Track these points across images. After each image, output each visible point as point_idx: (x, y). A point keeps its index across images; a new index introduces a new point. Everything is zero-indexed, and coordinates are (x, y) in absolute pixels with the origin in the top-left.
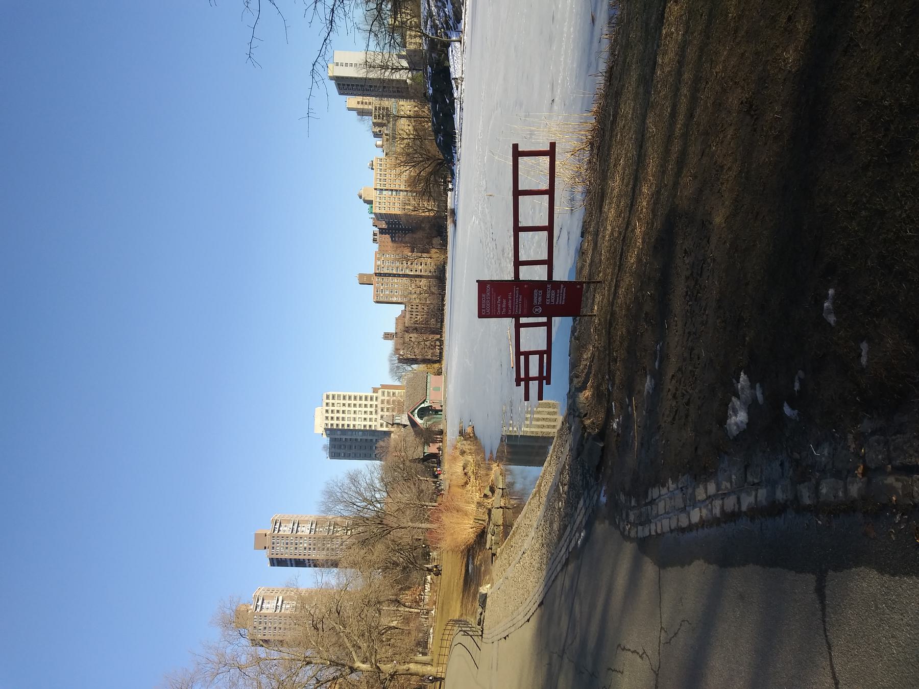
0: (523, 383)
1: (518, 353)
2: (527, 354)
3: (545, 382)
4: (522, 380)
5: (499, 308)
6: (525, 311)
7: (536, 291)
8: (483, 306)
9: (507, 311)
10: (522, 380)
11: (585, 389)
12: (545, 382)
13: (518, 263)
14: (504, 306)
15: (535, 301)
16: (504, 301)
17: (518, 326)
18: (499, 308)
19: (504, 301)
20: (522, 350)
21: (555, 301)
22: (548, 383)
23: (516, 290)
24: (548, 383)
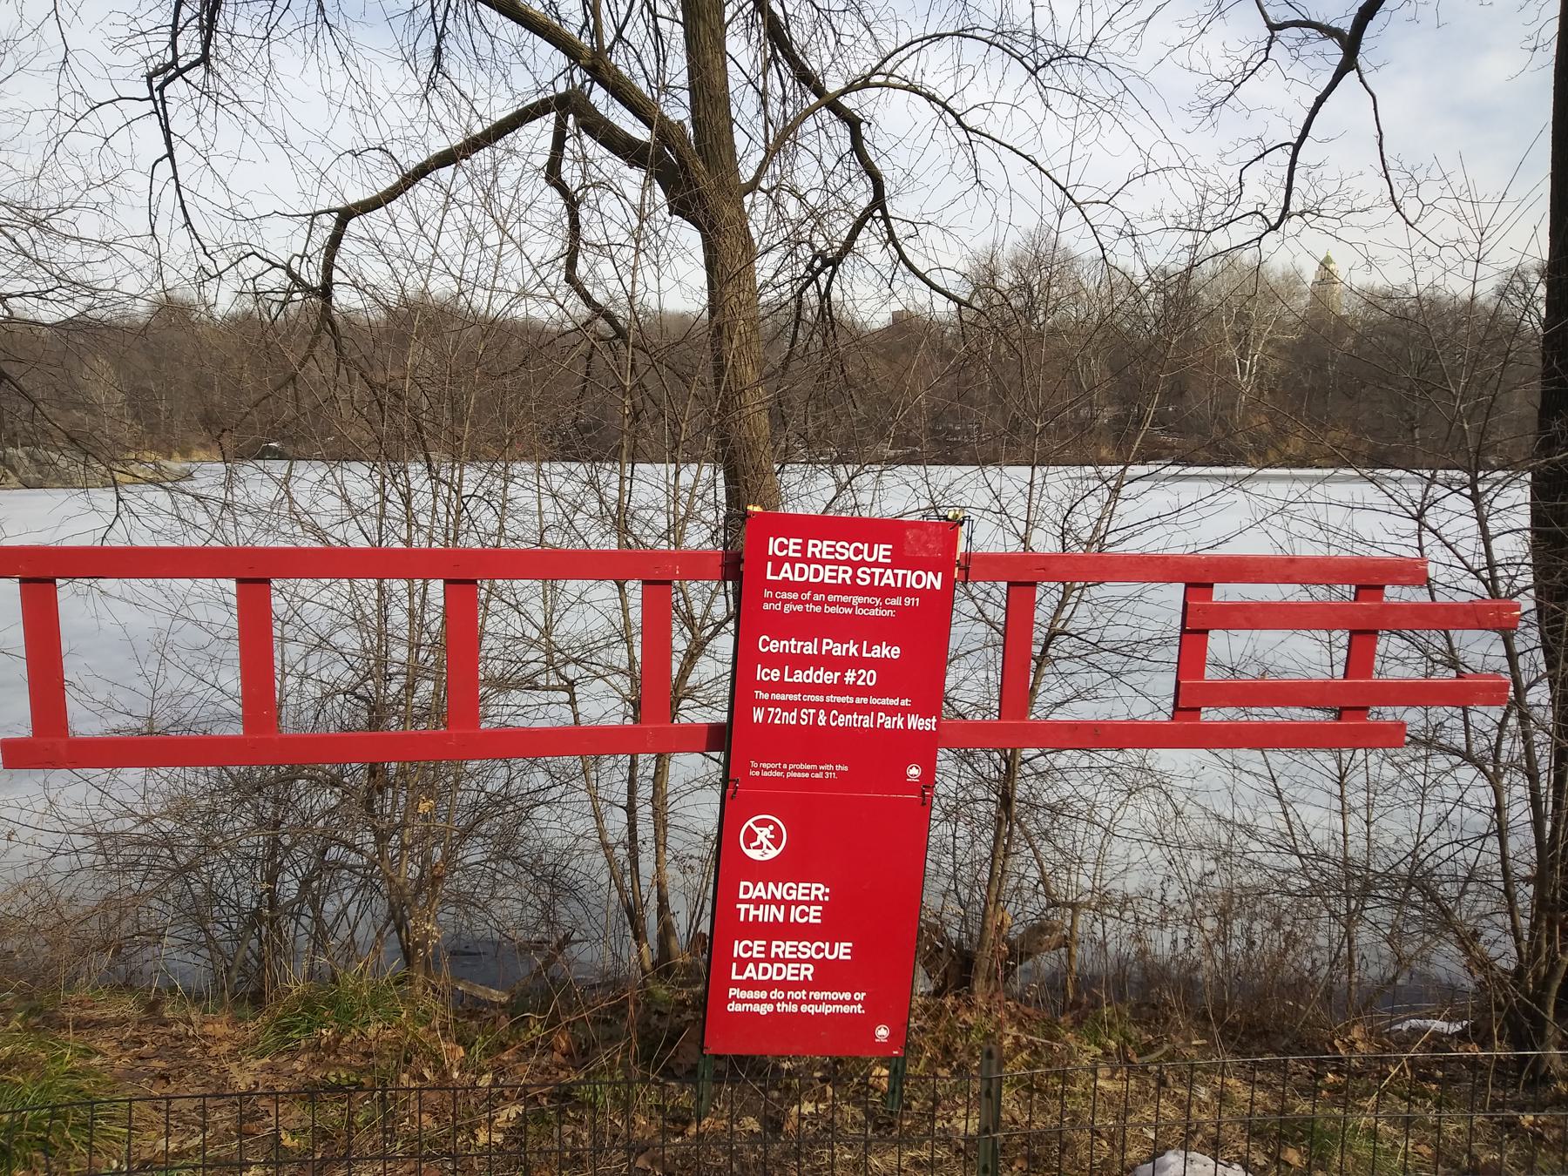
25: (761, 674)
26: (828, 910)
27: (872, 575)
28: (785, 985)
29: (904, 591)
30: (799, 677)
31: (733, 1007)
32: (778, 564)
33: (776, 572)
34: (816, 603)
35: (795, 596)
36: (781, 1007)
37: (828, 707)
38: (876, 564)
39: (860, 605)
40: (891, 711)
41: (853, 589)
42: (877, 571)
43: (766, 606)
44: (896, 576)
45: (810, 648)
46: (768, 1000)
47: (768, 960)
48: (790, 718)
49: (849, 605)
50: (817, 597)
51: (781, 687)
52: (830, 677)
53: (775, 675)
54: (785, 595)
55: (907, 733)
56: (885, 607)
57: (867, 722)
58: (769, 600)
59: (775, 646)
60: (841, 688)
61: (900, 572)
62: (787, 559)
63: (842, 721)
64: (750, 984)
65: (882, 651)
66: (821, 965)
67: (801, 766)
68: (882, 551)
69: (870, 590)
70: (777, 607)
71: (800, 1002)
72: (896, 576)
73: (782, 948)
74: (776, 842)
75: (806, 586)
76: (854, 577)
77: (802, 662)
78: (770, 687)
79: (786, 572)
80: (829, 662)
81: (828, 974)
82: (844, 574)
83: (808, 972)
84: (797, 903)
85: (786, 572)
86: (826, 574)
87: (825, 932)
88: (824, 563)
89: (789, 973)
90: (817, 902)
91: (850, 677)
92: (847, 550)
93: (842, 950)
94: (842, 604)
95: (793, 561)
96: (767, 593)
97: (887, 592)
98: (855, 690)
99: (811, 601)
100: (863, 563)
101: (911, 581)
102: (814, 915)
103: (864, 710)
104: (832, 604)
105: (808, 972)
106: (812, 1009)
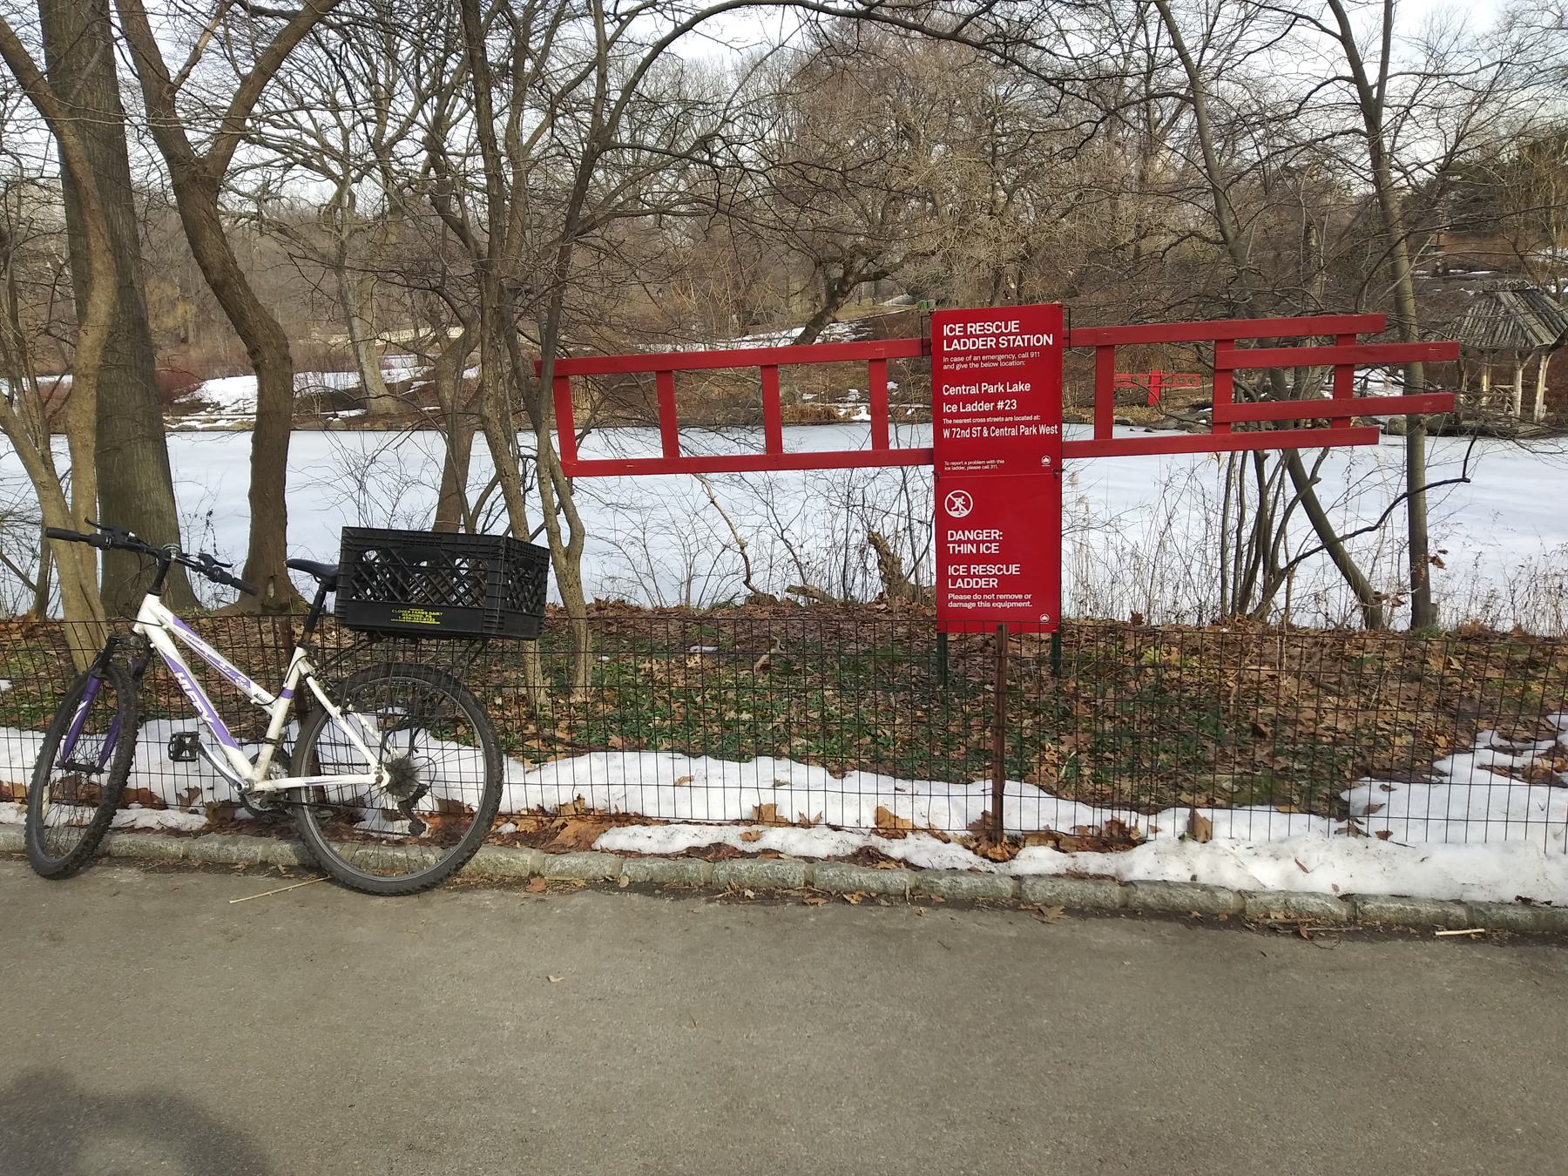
25: (946, 408)
26: (1002, 545)
28: (981, 591)
29: (1029, 349)
30: (969, 408)
31: (951, 605)
32: (950, 341)
36: (980, 604)
37: (988, 425)
38: (1011, 334)
40: (1028, 424)
41: (997, 351)
45: (974, 390)
46: (972, 601)
47: (969, 576)
48: (965, 434)
51: (959, 415)
52: (988, 407)
53: (954, 408)
55: (1039, 436)
57: (1014, 432)
59: (953, 391)
60: (995, 413)
62: (955, 337)
63: (998, 432)
64: (960, 591)
65: (1019, 387)
66: (1001, 578)
68: (1013, 326)
69: (1009, 350)
71: (991, 601)
73: (977, 569)
74: (967, 506)
75: (969, 352)
76: (997, 343)
77: (970, 399)
78: (952, 416)
80: (986, 397)
81: (1006, 584)
82: (991, 342)
83: (994, 583)
84: (983, 542)
85: (956, 345)
86: (980, 344)
87: (1002, 558)
88: (978, 337)
89: (982, 583)
90: (995, 540)
91: (1000, 405)
92: (991, 328)
93: (1014, 569)
95: (959, 338)
97: (1019, 350)
98: (1004, 413)
100: (1002, 334)
101: (1033, 341)
102: (994, 548)
103: (1011, 425)
105: (994, 583)
106: (1000, 605)
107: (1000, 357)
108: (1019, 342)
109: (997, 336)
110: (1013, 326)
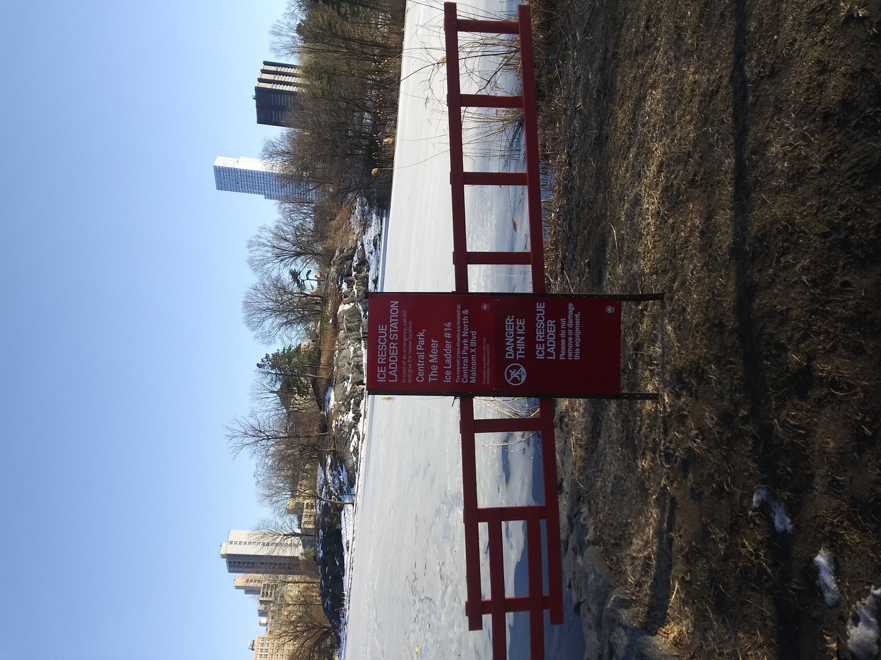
0: (487, 619)
1: (473, 514)
2: (497, 517)
3: (546, 613)
4: (486, 607)
5: (420, 365)
6: (487, 374)
7: (509, 321)
8: (381, 358)
9: (441, 373)
10: (486, 607)
11: (663, 622)
12: (546, 613)
13: (463, 258)
14: (434, 358)
15: (510, 350)
16: (434, 344)
17: (470, 427)
18: (420, 365)
19: (434, 344)
20: (483, 503)
21: (558, 350)
22: (557, 618)
23: (463, 314)
24: (557, 618)
27: (393, 333)
29: (400, 318)
33: (393, 378)
34: (407, 358)
35: (404, 368)
38: (388, 331)
39: (408, 337)
41: (400, 342)
42: (391, 330)
43: (410, 381)
44: (393, 322)
49: (408, 343)
50: (405, 358)
54: (404, 373)
56: (408, 326)
58: (407, 380)
61: (391, 320)
62: (387, 373)
67: (484, 360)
68: (382, 329)
69: (400, 333)
70: (410, 376)
72: (393, 322)
75: (400, 363)
76: (394, 341)
79: (393, 373)
85: (393, 373)
86: (394, 354)
94: (407, 346)
96: (404, 381)
97: (401, 326)
99: (406, 360)
100: (388, 338)
101: (395, 315)
104: (408, 351)
107: (405, 339)
108: (395, 325)
109: (389, 341)
110: (382, 329)
